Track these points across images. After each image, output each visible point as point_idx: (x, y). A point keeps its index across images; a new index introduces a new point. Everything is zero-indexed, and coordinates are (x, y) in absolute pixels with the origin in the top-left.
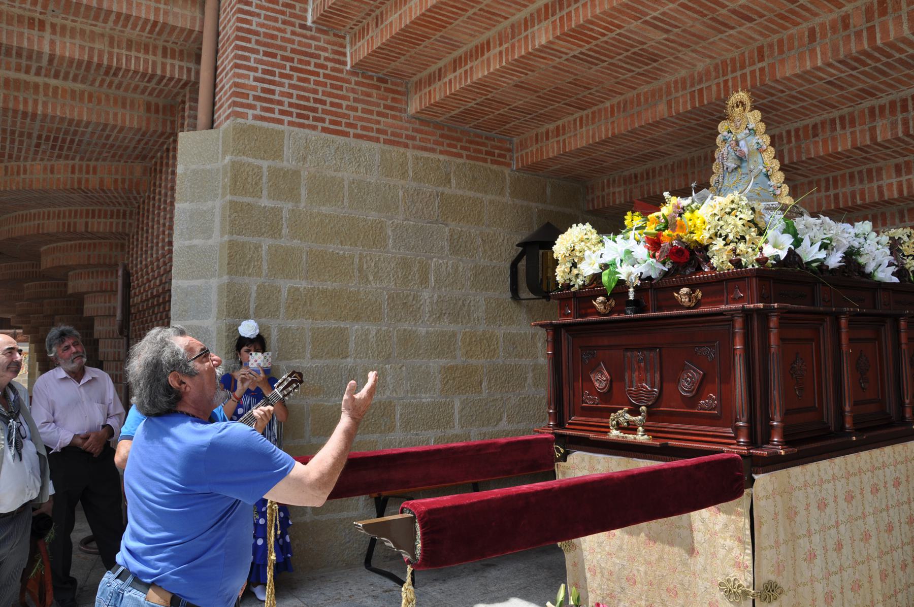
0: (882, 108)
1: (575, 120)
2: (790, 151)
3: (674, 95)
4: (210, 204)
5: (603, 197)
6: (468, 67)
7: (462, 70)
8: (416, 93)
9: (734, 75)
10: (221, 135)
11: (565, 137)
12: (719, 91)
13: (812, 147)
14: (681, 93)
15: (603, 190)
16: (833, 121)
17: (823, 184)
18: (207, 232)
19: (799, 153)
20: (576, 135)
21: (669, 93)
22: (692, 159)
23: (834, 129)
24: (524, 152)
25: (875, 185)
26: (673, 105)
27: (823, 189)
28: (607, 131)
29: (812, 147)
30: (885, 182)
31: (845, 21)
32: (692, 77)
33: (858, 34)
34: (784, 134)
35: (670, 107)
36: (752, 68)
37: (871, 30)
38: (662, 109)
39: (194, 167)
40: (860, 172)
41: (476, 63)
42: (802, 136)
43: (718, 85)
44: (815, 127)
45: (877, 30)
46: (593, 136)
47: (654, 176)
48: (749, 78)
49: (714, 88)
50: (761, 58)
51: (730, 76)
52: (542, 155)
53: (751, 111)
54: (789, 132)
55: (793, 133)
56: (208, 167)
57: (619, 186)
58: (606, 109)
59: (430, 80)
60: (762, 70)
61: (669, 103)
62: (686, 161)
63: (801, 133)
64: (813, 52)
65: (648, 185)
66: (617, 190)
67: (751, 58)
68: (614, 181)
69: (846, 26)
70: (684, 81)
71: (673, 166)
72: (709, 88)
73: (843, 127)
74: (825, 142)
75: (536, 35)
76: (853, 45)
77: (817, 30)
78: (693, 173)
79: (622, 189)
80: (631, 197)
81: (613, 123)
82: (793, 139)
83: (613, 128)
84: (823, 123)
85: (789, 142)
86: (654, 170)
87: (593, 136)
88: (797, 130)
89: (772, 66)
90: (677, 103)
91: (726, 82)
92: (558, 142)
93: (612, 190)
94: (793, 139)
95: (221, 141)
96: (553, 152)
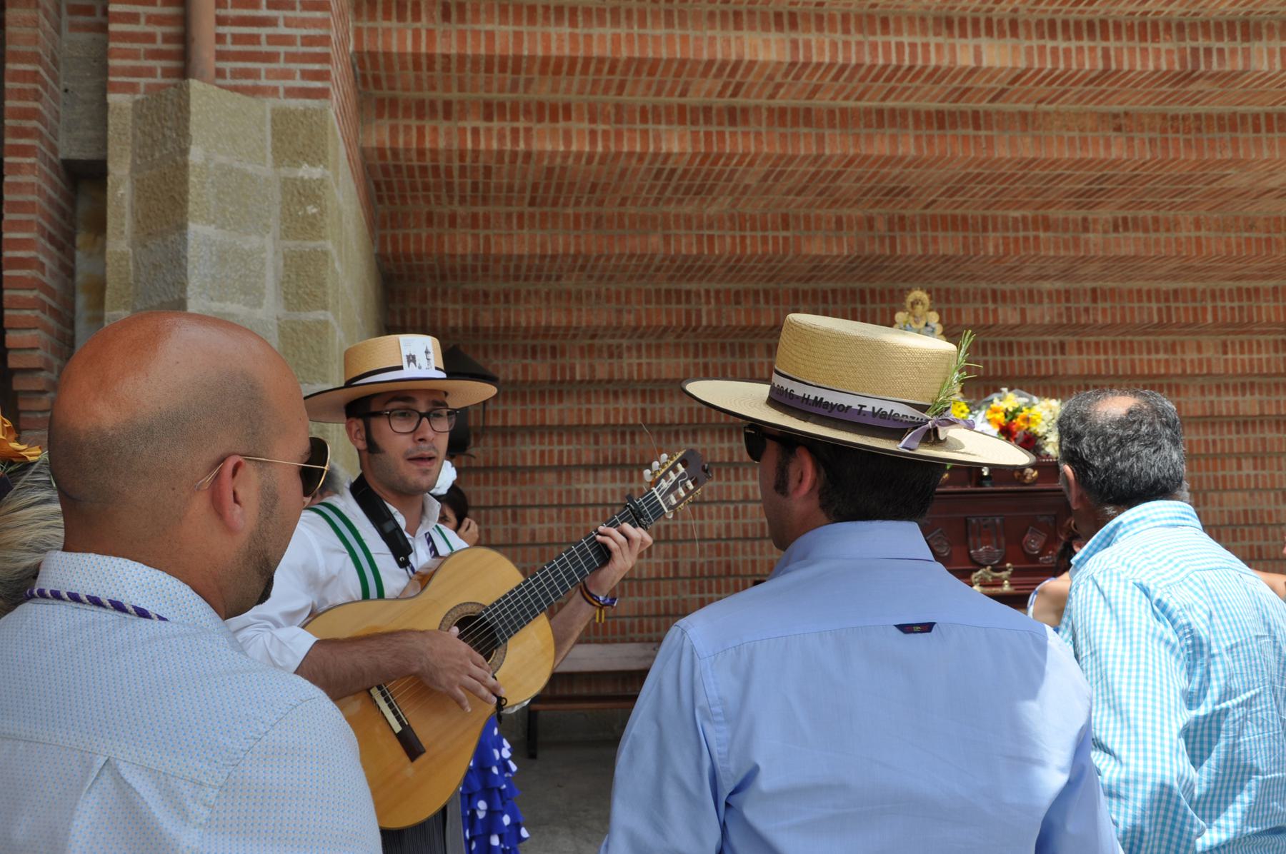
0: (805, 293)
1: (509, 216)
2: (709, 313)
3: (673, 231)
4: (254, 241)
5: (424, 312)
6: (521, 124)
7: (508, 125)
8: (380, 115)
9: (753, 233)
10: (269, 116)
11: (490, 232)
12: (734, 244)
13: (733, 314)
14: (682, 232)
15: (424, 300)
16: (756, 293)
17: (691, 349)
18: (252, 293)
19: (719, 316)
20: (510, 235)
21: (666, 226)
22: (579, 292)
23: (757, 301)
24: (400, 233)
25: (747, 361)
26: (673, 242)
27: (691, 354)
28: (567, 245)
29: (733, 314)
30: (756, 360)
31: (870, 222)
32: (700, 218)
33: (882, 239)
34: (703, 293)
35: (667, 243)
36: (776, 234)
37: (893, 239)
38: (655, 242)
39: (222, 159)
40: (732, 345)
41: (539, 126)
42: (723, 299)
43: (733, 238)
44: (737, 293)
45: (898, 241)
46: (543, 245)
47: (517, 300)
48: (770, 242)
49: (728, 240)
50: (786, 226)
51: (748, 233)
52: (441, 244)
53: (930, 310)
54: (708, 292)
55: (712, 294)
56: (250, 168)
57: (455, 302)
58: (566, 216)
59: (422, 109)
60: (786, 239)
61: (667, 238)
62: (569, 293)
63: (722, 296)
64: (840, 239)
65: (507, 310)
66: (450, 306)
67: (774, 222)
68: (445, 293)
69: (871, 227)
70: (688, 219)
71: (548, 294)
72: (722, 237)
73: (767, 302)
74: (748, 312)
75: (664, 136)
76: (877, 246)
77: (844, 220)
78: (580, 310)
79: (459, 307)
80: (475, 321)
81: (577, 237)
82: (713, 301)
83: (578, 244)
84: (747, 292)
85: (708, 302)
86: (517, 293)
87: (543, 245)
88: (717, 292)
89: (797, 238)
90: (678, 241)
91: (743, 238)
92: (476, 237)
93: (440, 304)
94: (713, 301)
95: (268, 129)
96: (465, 247)
